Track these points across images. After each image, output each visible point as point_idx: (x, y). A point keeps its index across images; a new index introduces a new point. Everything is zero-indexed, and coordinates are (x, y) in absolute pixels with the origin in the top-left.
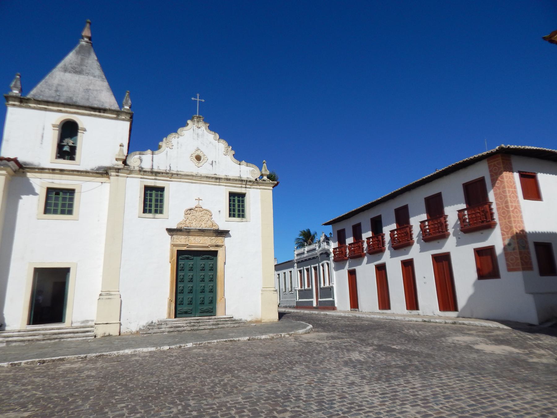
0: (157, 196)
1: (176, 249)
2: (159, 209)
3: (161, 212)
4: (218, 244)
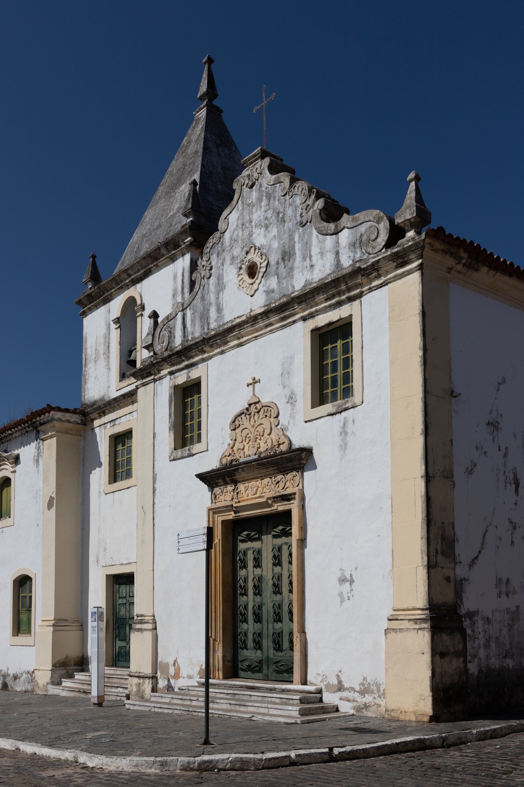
1: (219, 519)
4: (288, 491)
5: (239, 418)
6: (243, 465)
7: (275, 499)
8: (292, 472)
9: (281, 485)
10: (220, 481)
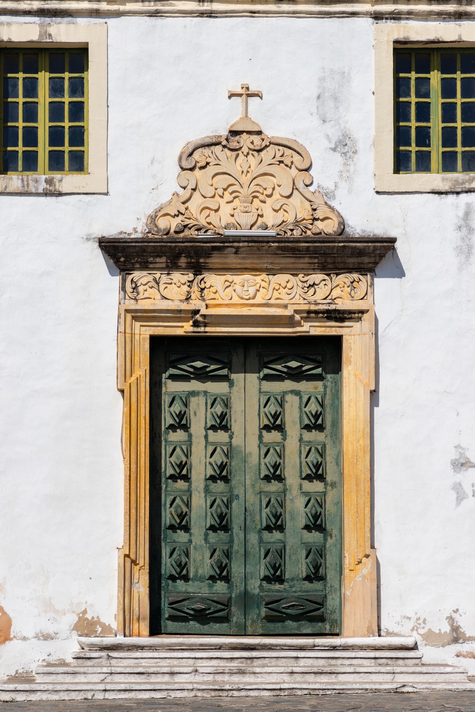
0: (56, 88)
2: (67, 148)
3: (78, 163)
5: (207, 151)
6: (246, 244)
7: (313, 315)
8: (350, 272)
9: (322, 292)
10: (164, 259)
